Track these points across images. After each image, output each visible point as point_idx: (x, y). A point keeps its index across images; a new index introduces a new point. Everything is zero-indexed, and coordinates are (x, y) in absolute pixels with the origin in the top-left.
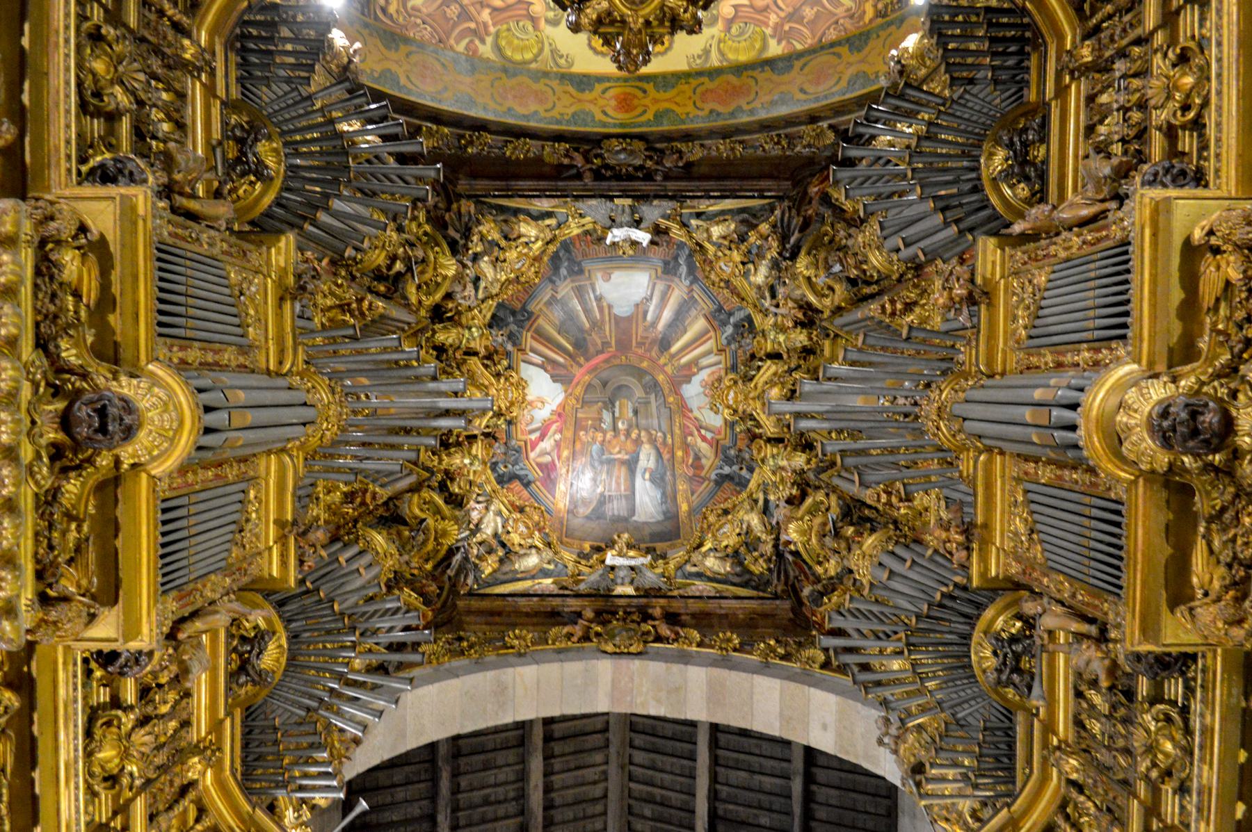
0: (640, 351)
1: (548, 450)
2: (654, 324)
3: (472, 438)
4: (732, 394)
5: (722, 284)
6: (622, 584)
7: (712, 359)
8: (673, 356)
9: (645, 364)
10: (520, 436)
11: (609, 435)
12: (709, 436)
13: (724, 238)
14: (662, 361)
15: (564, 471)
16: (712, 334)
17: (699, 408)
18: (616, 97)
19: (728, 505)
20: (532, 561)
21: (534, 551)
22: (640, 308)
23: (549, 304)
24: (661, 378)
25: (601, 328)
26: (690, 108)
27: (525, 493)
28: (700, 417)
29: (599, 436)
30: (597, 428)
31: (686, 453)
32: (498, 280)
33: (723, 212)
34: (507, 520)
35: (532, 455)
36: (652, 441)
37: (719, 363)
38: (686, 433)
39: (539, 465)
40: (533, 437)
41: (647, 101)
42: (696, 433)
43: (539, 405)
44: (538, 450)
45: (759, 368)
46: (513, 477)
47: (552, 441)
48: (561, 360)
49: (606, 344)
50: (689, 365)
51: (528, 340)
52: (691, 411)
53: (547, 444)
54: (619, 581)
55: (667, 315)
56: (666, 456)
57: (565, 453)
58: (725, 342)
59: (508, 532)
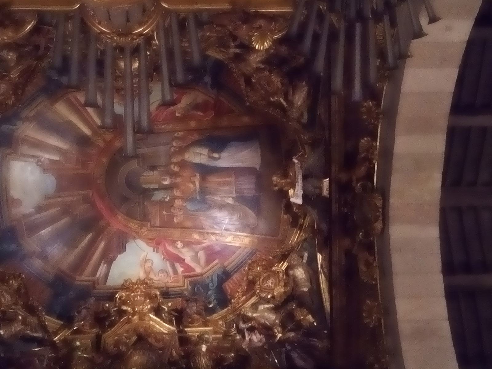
1: (193, 254)
3: (184, 340)
6: (321, 189)
8: (95, 132)
9: (105, 160)
10: (180, 283)
11: (177, 193)
14: (100, 143)
15: (213, 238)
19: (242, 82)
20: (300, 273)
21: (291, 272)
27: (236, 277)
29: (178, 203)
30: (170, 205)
32: (24, 319)
34: (261, 298)
35: (198, 270)
36: (181, 150)
40: (180, 269)
43: (148, 264)
44: (192, 264)
46: (220, 289)
47: (185, 250)
48: (102, 244)
49: (86, 200)
51: (84, 278)
53: (187, 255)
54: (317, 191)
55: (54, 141)
57: (196, 236)
59: (273, 297)
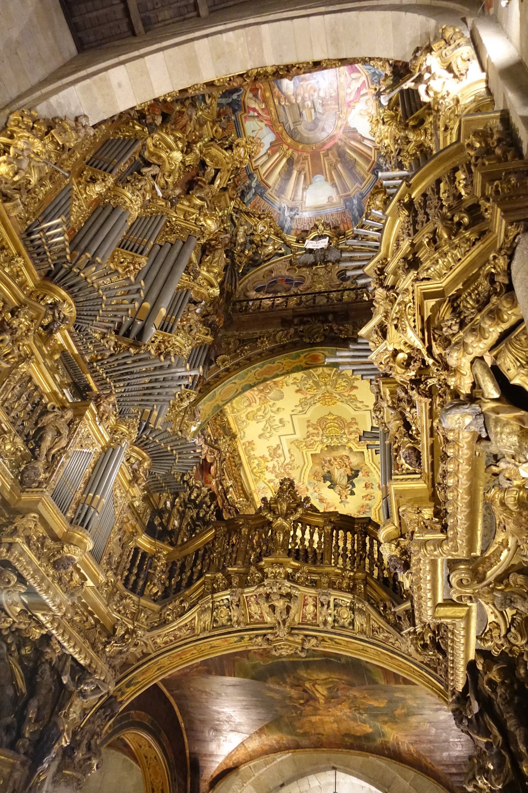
0: (305, 154)
2: (299, 173)
4: (242, 155)
5: (262, 216)
7: (260, 162)
8: (284, 156)
12: (252, 113)
13: (266, 246)
16: (263, 178)
17: (261, 129)
18: (319, 360)
22: (308, 183)
23: (364, 179)
24: (289, 140)
25: (331, 165)
26: (284, 362)
28: (259, 123)
29: (322, 94)
31: (264, 97)
33: (269, 260)
35: (364, 78)
36: (287, 98)
37: (255, 161)
38: (267, 110)
39: (358, 71)
40: (364, 91)
41: (305, 360)
42: (260, 112)
43: (363, 113)
44: (361, 82)
45: (229, 180)
47: (352, 87)
48: (353, 143)
49: (326, 155)
50: (274, 153)
52: (266, 125)
53: (356, 85)
56: (276, 90)
58: (255, 175)
